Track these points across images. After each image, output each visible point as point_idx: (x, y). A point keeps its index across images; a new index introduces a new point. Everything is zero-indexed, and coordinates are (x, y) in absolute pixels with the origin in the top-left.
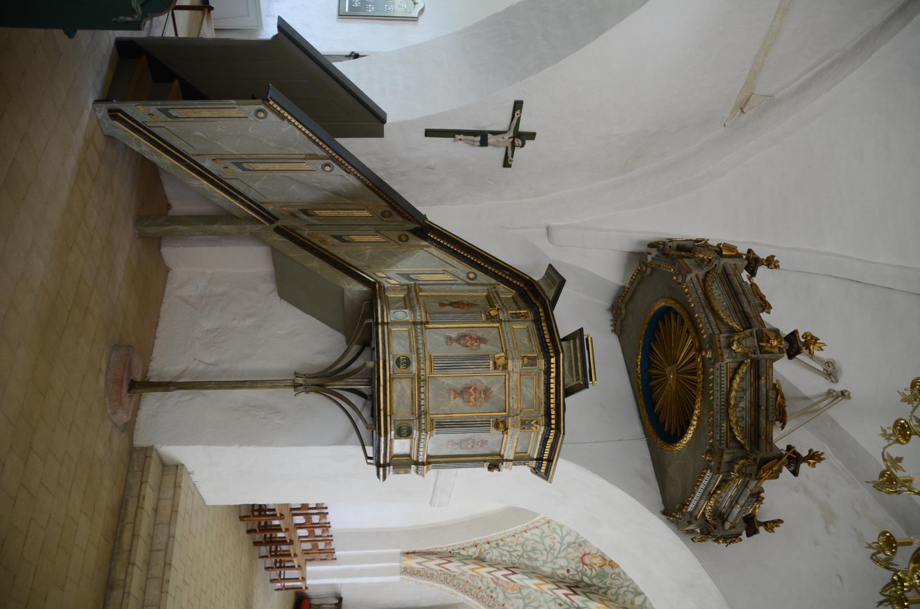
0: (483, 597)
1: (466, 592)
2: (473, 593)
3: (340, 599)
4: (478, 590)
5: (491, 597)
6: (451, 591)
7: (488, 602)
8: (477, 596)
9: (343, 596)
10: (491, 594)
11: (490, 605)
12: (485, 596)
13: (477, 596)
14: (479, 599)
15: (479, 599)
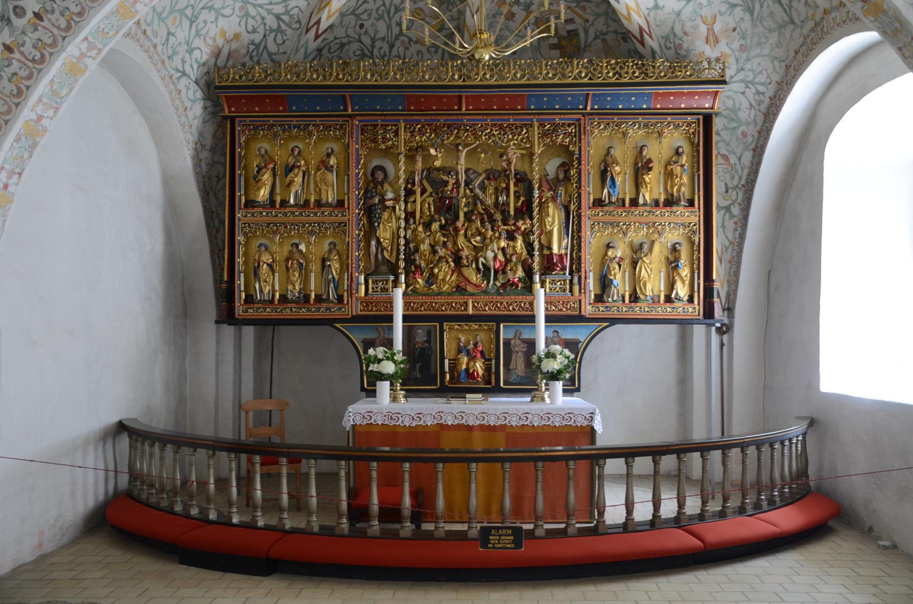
0: (38, 44)
1: (20, 93)
2: (24, 73)
3: (121, 427)
4: (17, 55)
5: (37, 15)
6: (17, 140)
7: (55, 31)
8: (33, 61)
9: (114, 419)
10: (30, 15)
11: (63, 24)
12: (36, 35)
13: (33, 61)
14: (43, 56)
15: (43, 56)
